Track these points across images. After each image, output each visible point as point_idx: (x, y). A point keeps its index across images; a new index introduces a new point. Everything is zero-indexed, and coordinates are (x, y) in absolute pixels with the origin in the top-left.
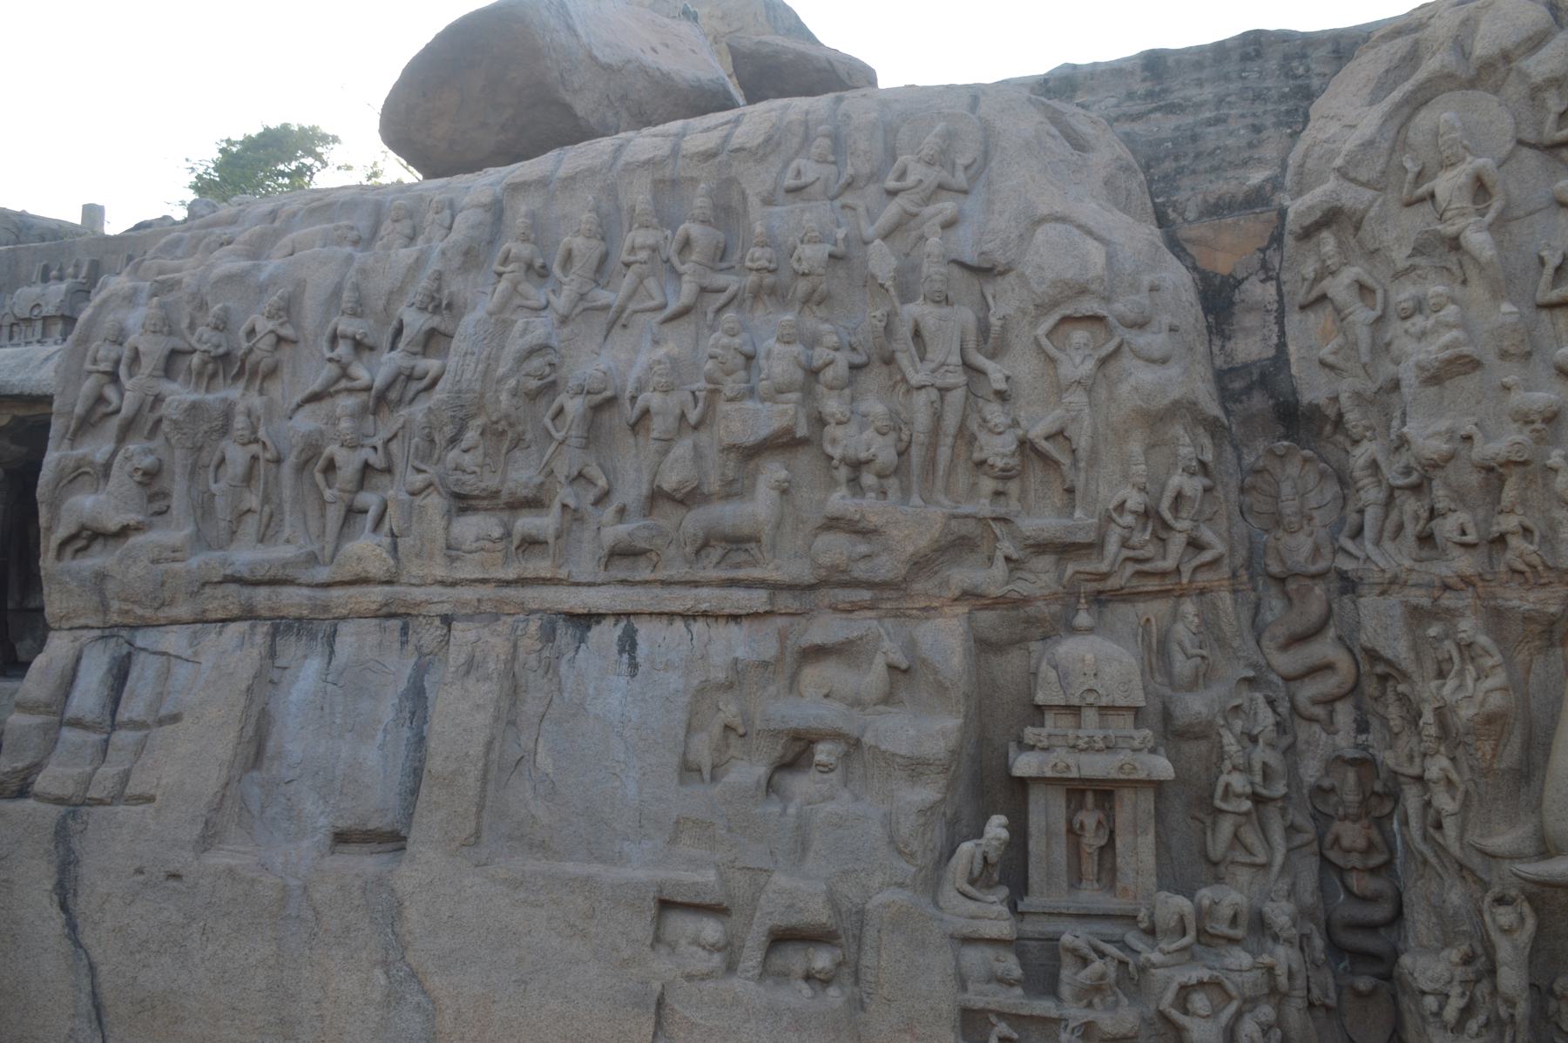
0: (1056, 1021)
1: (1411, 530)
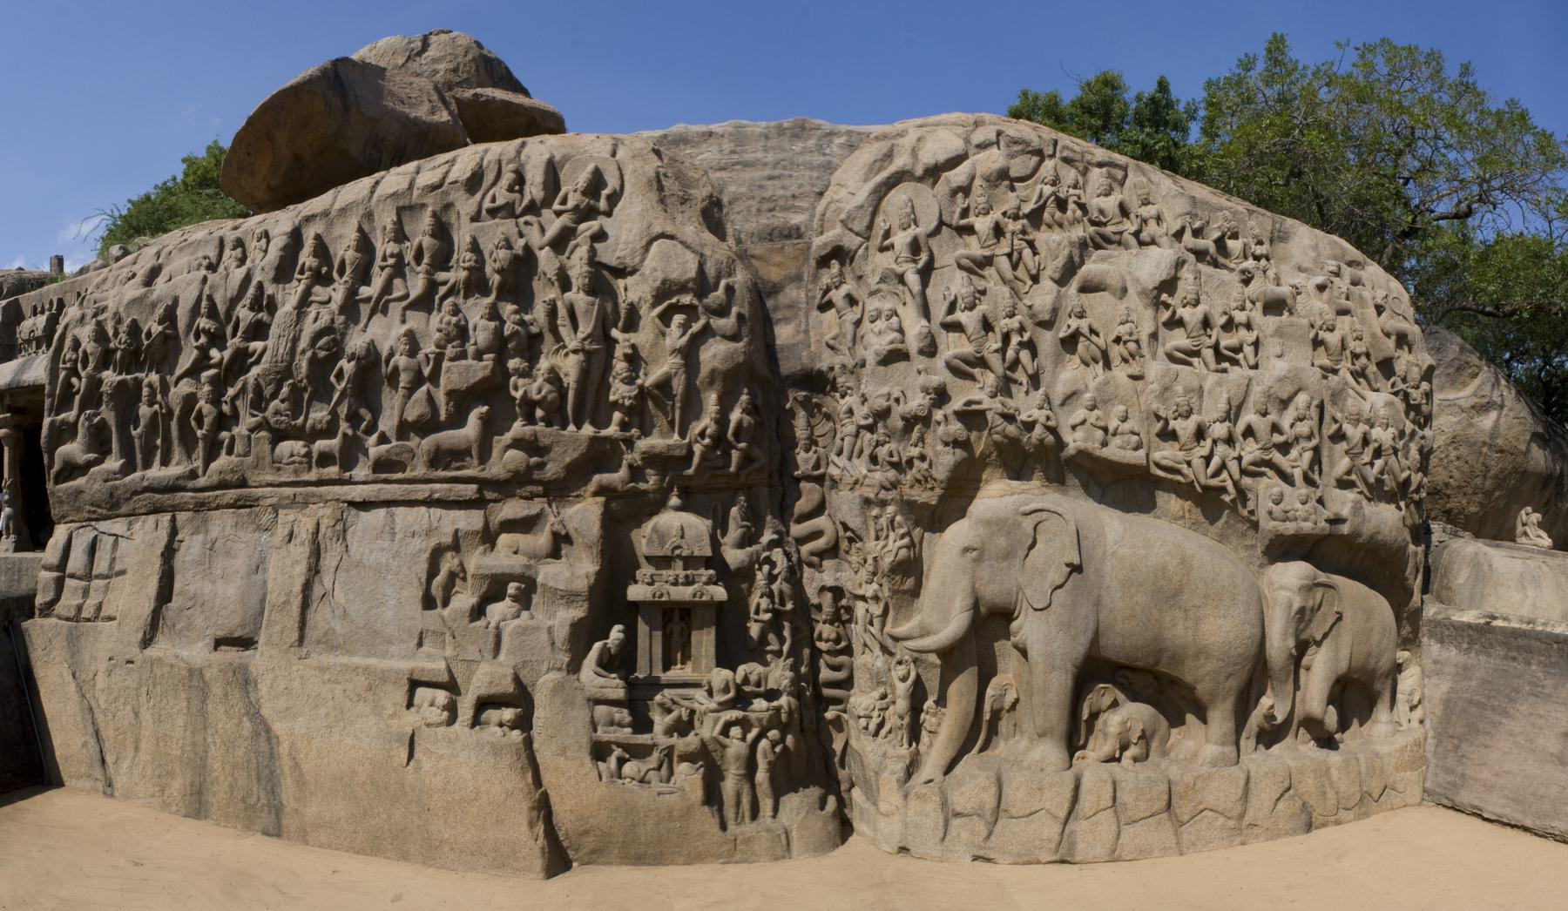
0: (655, 745)
1: (867, 452)
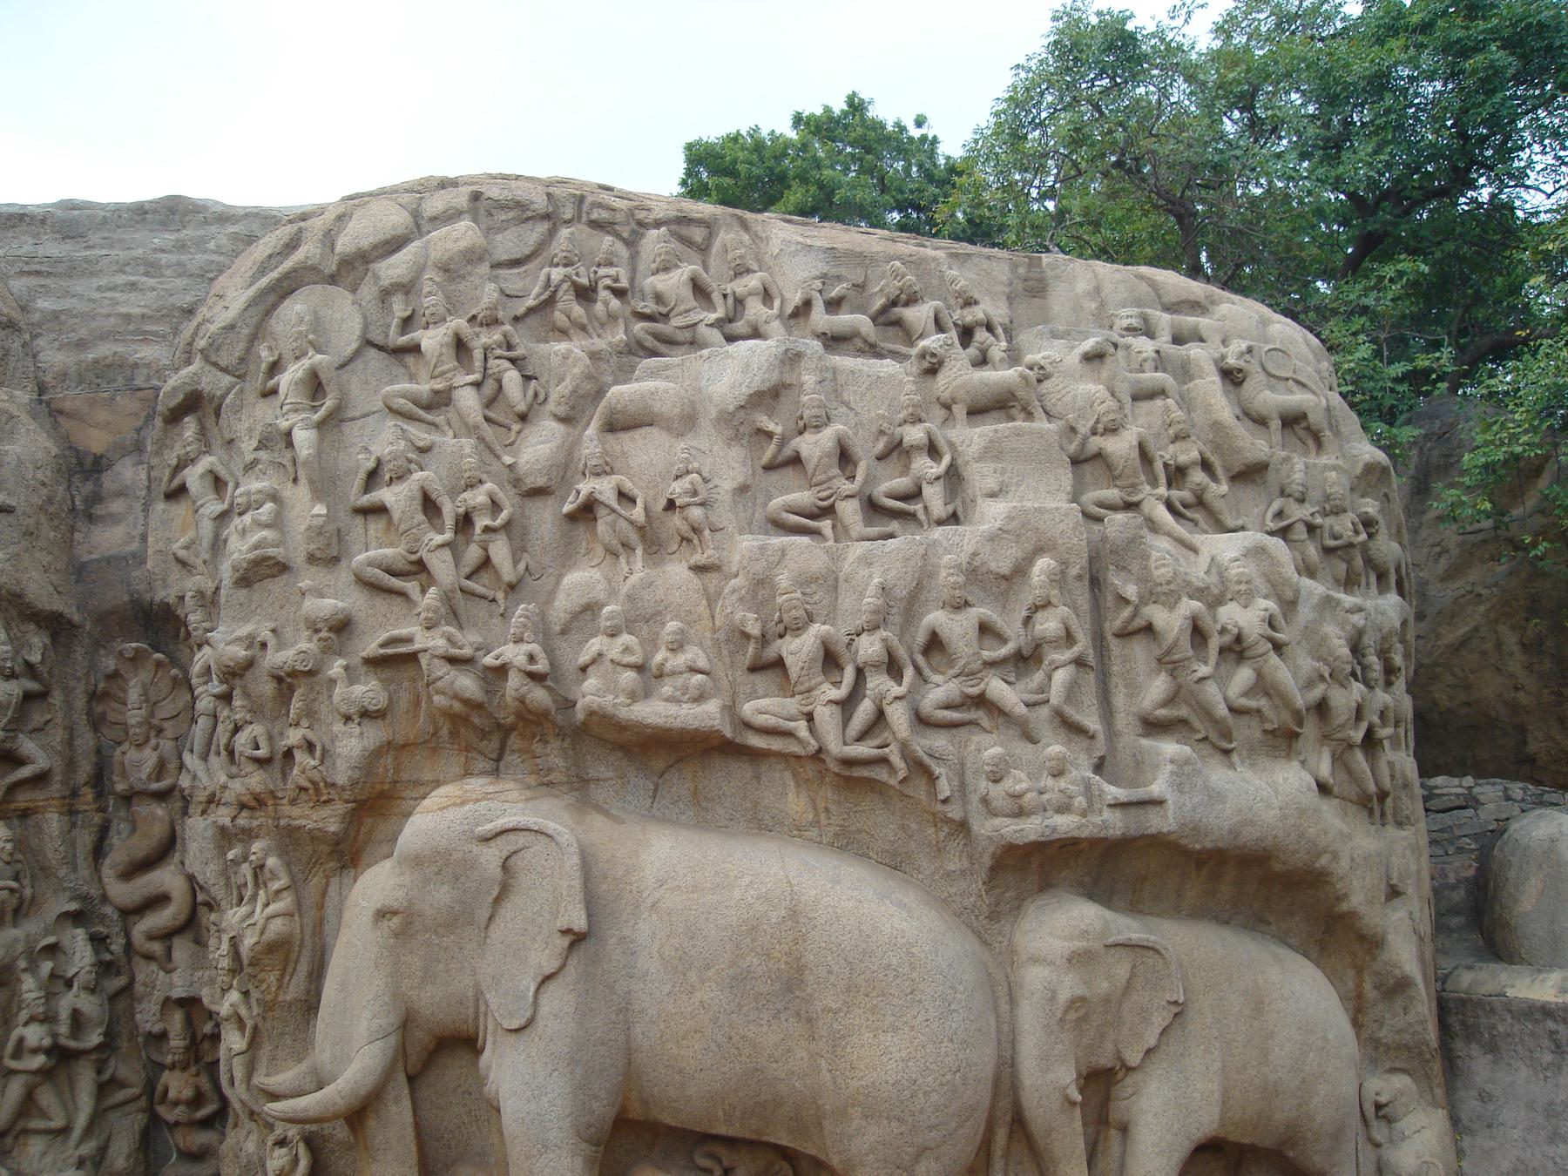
1: (223, 741)
